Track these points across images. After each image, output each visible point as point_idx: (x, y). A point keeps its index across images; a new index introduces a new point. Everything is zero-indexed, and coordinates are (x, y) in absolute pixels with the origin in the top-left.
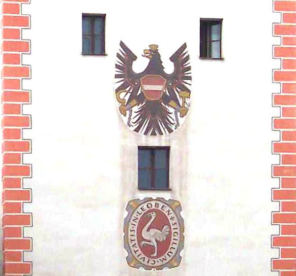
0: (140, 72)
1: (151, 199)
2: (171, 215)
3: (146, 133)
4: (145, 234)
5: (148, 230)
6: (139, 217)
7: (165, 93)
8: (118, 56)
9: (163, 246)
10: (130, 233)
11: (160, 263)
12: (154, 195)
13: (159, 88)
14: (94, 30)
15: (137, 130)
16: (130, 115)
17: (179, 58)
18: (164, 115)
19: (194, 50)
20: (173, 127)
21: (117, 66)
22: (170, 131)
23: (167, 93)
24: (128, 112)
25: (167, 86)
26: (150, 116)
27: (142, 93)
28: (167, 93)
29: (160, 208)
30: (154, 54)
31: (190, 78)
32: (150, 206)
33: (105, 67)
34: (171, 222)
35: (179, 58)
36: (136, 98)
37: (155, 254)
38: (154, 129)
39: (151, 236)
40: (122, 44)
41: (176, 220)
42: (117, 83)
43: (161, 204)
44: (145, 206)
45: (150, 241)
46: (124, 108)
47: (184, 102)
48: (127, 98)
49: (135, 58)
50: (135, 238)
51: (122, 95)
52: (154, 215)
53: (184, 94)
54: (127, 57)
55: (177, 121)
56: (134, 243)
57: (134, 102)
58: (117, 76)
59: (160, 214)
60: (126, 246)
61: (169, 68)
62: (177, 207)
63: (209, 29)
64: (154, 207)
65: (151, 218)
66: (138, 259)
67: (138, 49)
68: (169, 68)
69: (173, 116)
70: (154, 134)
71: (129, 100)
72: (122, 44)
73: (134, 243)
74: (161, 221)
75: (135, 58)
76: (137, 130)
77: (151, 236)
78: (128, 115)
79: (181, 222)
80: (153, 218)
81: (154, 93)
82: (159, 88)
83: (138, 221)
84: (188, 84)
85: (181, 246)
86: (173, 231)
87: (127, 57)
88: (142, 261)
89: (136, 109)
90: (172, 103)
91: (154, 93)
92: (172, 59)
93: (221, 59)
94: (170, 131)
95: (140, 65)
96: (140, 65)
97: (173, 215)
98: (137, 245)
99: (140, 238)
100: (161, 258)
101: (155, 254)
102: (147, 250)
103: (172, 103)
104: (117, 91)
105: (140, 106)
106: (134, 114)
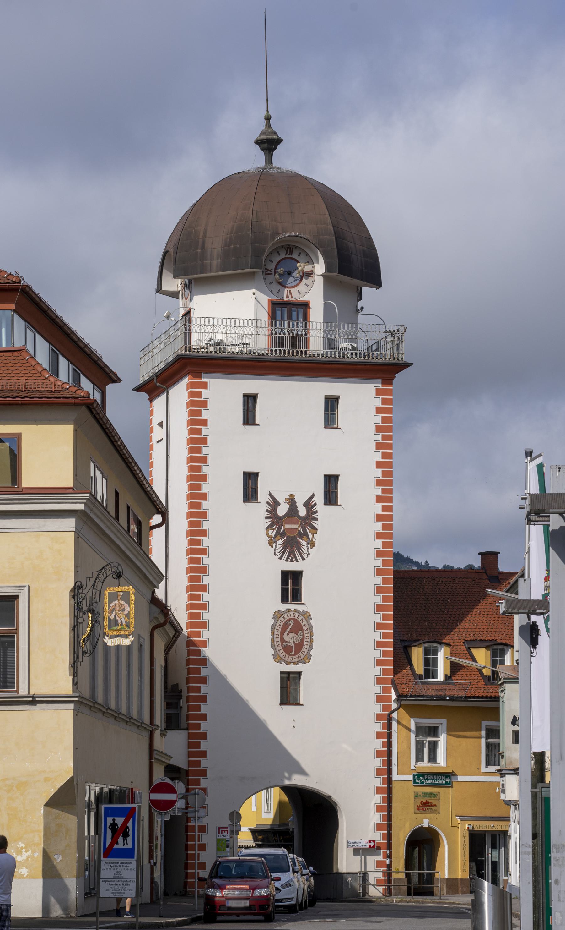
0: (103, 360)
1: (289, 611)
2: (304, 623)
3: (286, 561)
4: (286, 638)
5: (288, 635)
6: (282, 624)
7: (300, 531)
8: (268, 503)
9: (299, 646)
10: (275, 636)
11: (297, 660)
12: (293, 607)
13: (295, 527)
16: (276, 547)
17: (309, 505)
19: (319, 499)
20: (305, 556)
21: (267, 511)
22: (303, 559)
24: (274, 545)
25: (301, 525)
27: (284, 530)
29: (296, 618)
30: (292, 501)
31: (317, 519)
32: (289, 615)
33: (258, 512)
34: (304, 628)
35: (309, 505)
37: (293, 653)
38: (292, 558)
39: (291, 638)
40: (270, 494)
41: (307, 627)
43: (297, 615)
44: (286, 615)
45: (289, 642)
47: (313, 537)
48: (273, 534)
49: (279, 504)
50: (279, 640)
51: (270, 532)
52: (292, 623)
53: (313, 531)
54: (274, 504)
55: (308, 551)
56: (278, 644)
57: (279, 537)
58: (267, 518)
59: (296, 621)
60: (273, 646)
61: (302, 512)
62: (307, 616)
63: (331, 481)
64: (292, 617)
65: (290, 624)
66: (281, 656)
67: (281, 498)
68: (302, 512)
69: (305, 547)
70: (292, 561)
72: (270, 494)
73: (278, 644)
74: (297, 628)
75: (279, 504)
77: (291, 638)
78: (274, 547)
79: (311, 628)
80: (292, 624)
81: (292, 529)
82: (295, 527)
83: (281, 627)
84: (315, 523)
85: (311, 647)
86: (306, 635)
87: (274, 504)
88: (283, 658)
89: (280, 542)
90: (305, 537)
91: (292, 529)
92: (305, 505)
94: (303, 559)
95: (282, 510)
96: (282, 510)
97: (305, 623)
98: (280, 646)
99: (283, 640)
100: (297, 656)
101: (293, 653)
102: (287, 650)
103: (305, 537)
104: (268, 528)
105: (283, 540)
106: (278, 546)
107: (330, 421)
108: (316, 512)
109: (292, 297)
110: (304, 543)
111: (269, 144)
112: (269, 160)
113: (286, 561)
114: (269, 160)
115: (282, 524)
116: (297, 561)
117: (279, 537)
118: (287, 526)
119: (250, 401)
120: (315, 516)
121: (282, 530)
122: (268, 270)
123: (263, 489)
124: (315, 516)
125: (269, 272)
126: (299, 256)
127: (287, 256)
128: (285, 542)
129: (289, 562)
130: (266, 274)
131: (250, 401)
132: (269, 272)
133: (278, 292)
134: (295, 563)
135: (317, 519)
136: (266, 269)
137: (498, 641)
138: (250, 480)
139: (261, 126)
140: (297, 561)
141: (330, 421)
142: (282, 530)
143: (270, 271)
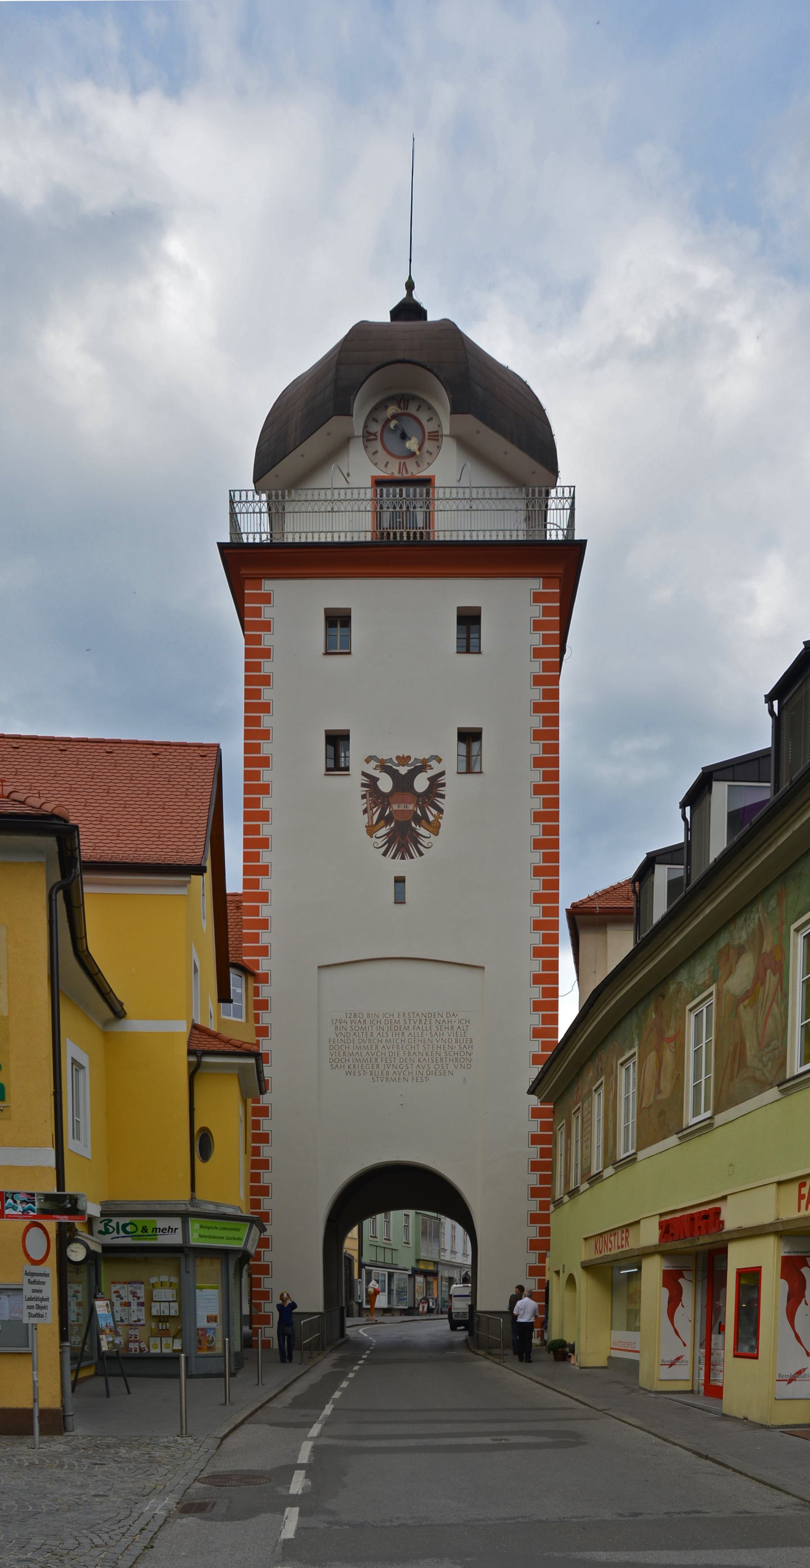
3: (394, 857)
7: (416, 812)
13: (411, 807)
15: (385, 854)
18: (415, 839)
21: (363, 785)
22: (421, 854)
23: (419, 812)
25: (417, 804)
26: (399, 838)
27: (390, 812)
28: (419, 812)
31: (443, 796)
33: (351, 785)
36: (384, 819)
38: (403, 852)
42: (362, 804)
46: (371, 830)
57: (382, 822)
70: (403, 858)
71: (377, 822)
76: (385, 854)
84: (440, 802)
89: (384, 831)
90: (423, 822)
93: (481, 772)
94: (421, 854)
95: (386, 784)
105: (388, 827)
108: (443, 785)
109: (407, 472)
110: (422, 831)
113: (394, 857)
115: (389, 805)
116: (412, 857)
117: (382, 822)
118: (395, 807)
120: (442, 790)
121: (388, 812)
122: (370, 434)
124: (442, 790)
125: (372, 437)
126: (418, 410)
127: (427, 435)
128: (392, 830)
129: (398, 860)
130: (368, 440)
132: (372, 437)
133: (386, 466)
134: (408, 860)
135: (443, 796)
136: (368, 432)
137: (731, 1049)
138: (337, 741)
140: (412, 857)
142: (388, 812)
143: (375, 435)
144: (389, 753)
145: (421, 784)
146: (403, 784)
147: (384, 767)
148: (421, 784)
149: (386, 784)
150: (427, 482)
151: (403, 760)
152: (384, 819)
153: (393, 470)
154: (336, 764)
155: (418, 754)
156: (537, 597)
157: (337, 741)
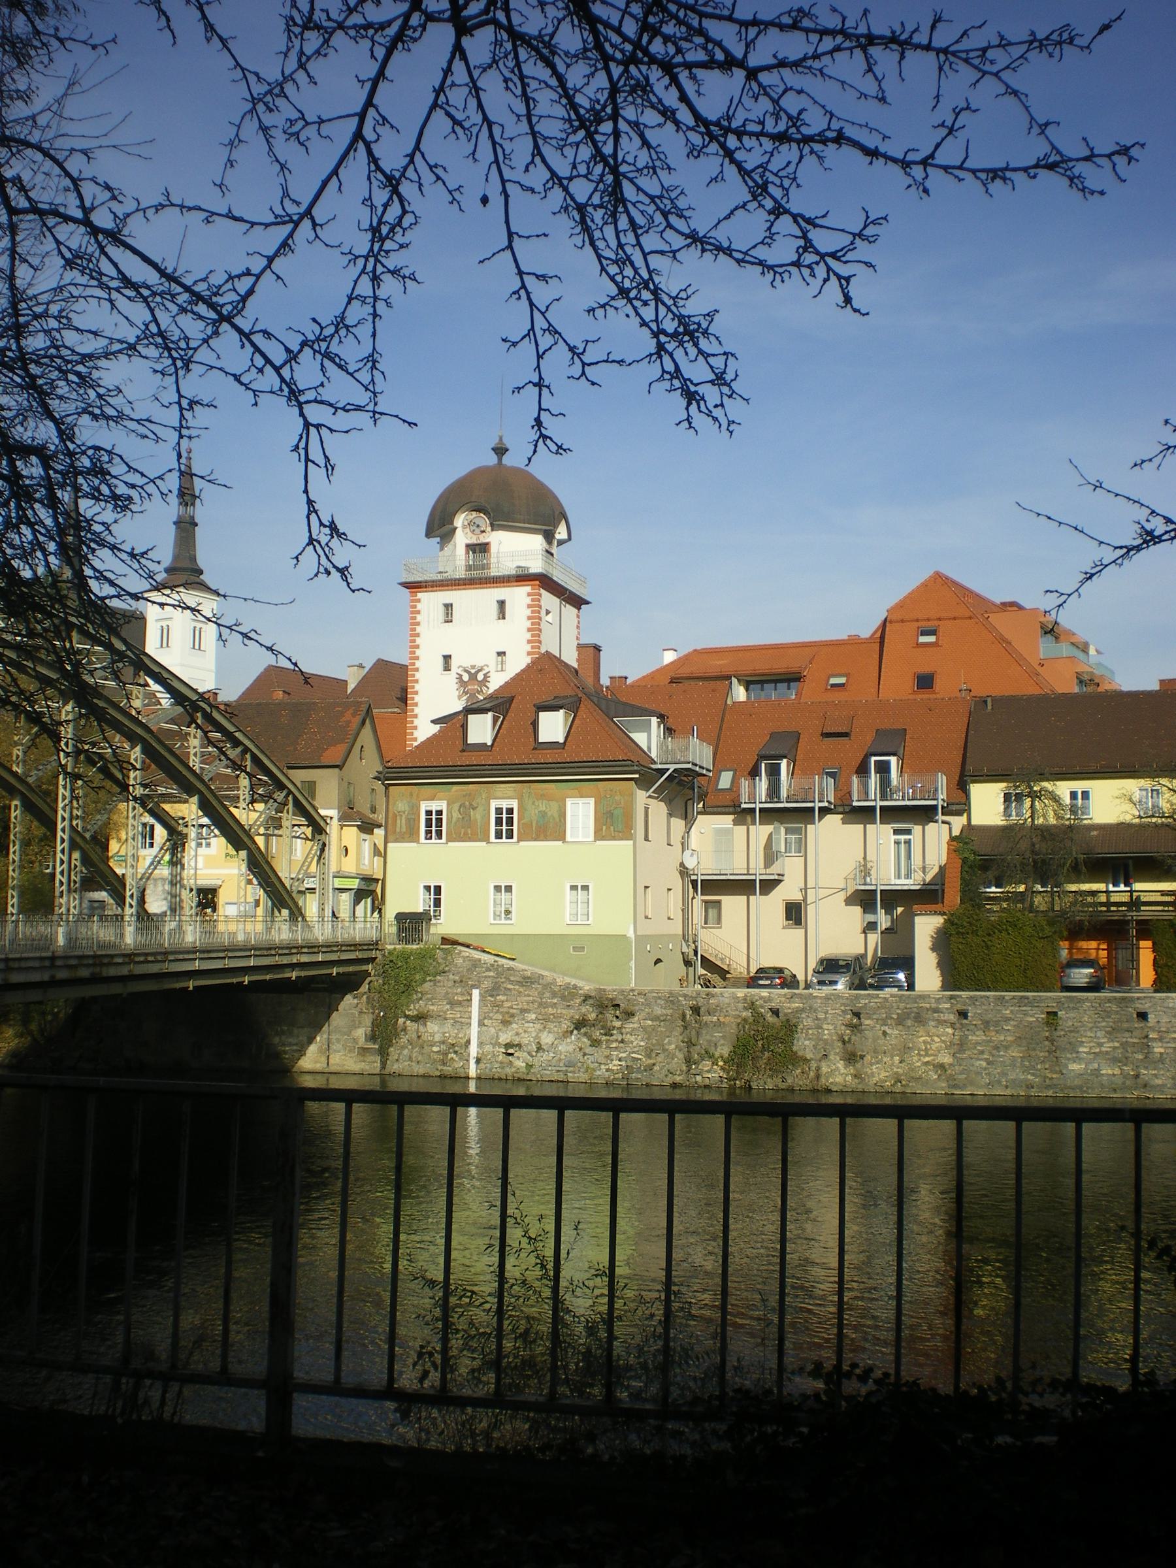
14: (447, 658)
33: (451, 678)
36: (465, 693)
42: (456, 686)
46: (459, 697)
95: (466, 677)
107: (502, 614)
111: (500, 451)
112: (500, 460)
114: (500, 460)
119: (448, 607)
123: (454, 663)
131: (448, 607)
139: (497, 441)
141: (502, 614)
144: (467, 664)
145: (480, 677)
146: (473, 677)
147: (466, 671)
148: (480, 677)
149: (466, 677)
150: (487, 544)
151: (473, 667)
152: (465, 693)
153: (474, 540)
154: (447, 668)
155: (479, 664)
156: (529, 594)
157: (447, 658)
